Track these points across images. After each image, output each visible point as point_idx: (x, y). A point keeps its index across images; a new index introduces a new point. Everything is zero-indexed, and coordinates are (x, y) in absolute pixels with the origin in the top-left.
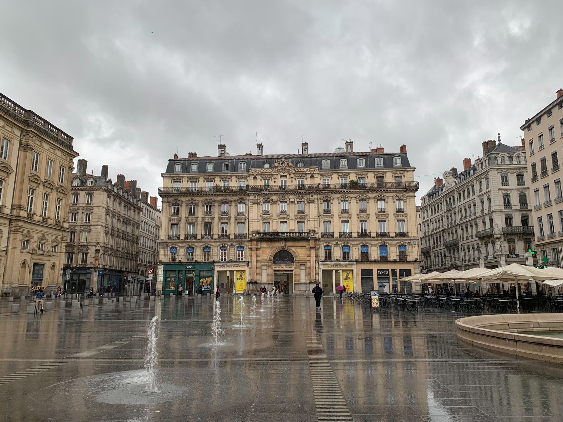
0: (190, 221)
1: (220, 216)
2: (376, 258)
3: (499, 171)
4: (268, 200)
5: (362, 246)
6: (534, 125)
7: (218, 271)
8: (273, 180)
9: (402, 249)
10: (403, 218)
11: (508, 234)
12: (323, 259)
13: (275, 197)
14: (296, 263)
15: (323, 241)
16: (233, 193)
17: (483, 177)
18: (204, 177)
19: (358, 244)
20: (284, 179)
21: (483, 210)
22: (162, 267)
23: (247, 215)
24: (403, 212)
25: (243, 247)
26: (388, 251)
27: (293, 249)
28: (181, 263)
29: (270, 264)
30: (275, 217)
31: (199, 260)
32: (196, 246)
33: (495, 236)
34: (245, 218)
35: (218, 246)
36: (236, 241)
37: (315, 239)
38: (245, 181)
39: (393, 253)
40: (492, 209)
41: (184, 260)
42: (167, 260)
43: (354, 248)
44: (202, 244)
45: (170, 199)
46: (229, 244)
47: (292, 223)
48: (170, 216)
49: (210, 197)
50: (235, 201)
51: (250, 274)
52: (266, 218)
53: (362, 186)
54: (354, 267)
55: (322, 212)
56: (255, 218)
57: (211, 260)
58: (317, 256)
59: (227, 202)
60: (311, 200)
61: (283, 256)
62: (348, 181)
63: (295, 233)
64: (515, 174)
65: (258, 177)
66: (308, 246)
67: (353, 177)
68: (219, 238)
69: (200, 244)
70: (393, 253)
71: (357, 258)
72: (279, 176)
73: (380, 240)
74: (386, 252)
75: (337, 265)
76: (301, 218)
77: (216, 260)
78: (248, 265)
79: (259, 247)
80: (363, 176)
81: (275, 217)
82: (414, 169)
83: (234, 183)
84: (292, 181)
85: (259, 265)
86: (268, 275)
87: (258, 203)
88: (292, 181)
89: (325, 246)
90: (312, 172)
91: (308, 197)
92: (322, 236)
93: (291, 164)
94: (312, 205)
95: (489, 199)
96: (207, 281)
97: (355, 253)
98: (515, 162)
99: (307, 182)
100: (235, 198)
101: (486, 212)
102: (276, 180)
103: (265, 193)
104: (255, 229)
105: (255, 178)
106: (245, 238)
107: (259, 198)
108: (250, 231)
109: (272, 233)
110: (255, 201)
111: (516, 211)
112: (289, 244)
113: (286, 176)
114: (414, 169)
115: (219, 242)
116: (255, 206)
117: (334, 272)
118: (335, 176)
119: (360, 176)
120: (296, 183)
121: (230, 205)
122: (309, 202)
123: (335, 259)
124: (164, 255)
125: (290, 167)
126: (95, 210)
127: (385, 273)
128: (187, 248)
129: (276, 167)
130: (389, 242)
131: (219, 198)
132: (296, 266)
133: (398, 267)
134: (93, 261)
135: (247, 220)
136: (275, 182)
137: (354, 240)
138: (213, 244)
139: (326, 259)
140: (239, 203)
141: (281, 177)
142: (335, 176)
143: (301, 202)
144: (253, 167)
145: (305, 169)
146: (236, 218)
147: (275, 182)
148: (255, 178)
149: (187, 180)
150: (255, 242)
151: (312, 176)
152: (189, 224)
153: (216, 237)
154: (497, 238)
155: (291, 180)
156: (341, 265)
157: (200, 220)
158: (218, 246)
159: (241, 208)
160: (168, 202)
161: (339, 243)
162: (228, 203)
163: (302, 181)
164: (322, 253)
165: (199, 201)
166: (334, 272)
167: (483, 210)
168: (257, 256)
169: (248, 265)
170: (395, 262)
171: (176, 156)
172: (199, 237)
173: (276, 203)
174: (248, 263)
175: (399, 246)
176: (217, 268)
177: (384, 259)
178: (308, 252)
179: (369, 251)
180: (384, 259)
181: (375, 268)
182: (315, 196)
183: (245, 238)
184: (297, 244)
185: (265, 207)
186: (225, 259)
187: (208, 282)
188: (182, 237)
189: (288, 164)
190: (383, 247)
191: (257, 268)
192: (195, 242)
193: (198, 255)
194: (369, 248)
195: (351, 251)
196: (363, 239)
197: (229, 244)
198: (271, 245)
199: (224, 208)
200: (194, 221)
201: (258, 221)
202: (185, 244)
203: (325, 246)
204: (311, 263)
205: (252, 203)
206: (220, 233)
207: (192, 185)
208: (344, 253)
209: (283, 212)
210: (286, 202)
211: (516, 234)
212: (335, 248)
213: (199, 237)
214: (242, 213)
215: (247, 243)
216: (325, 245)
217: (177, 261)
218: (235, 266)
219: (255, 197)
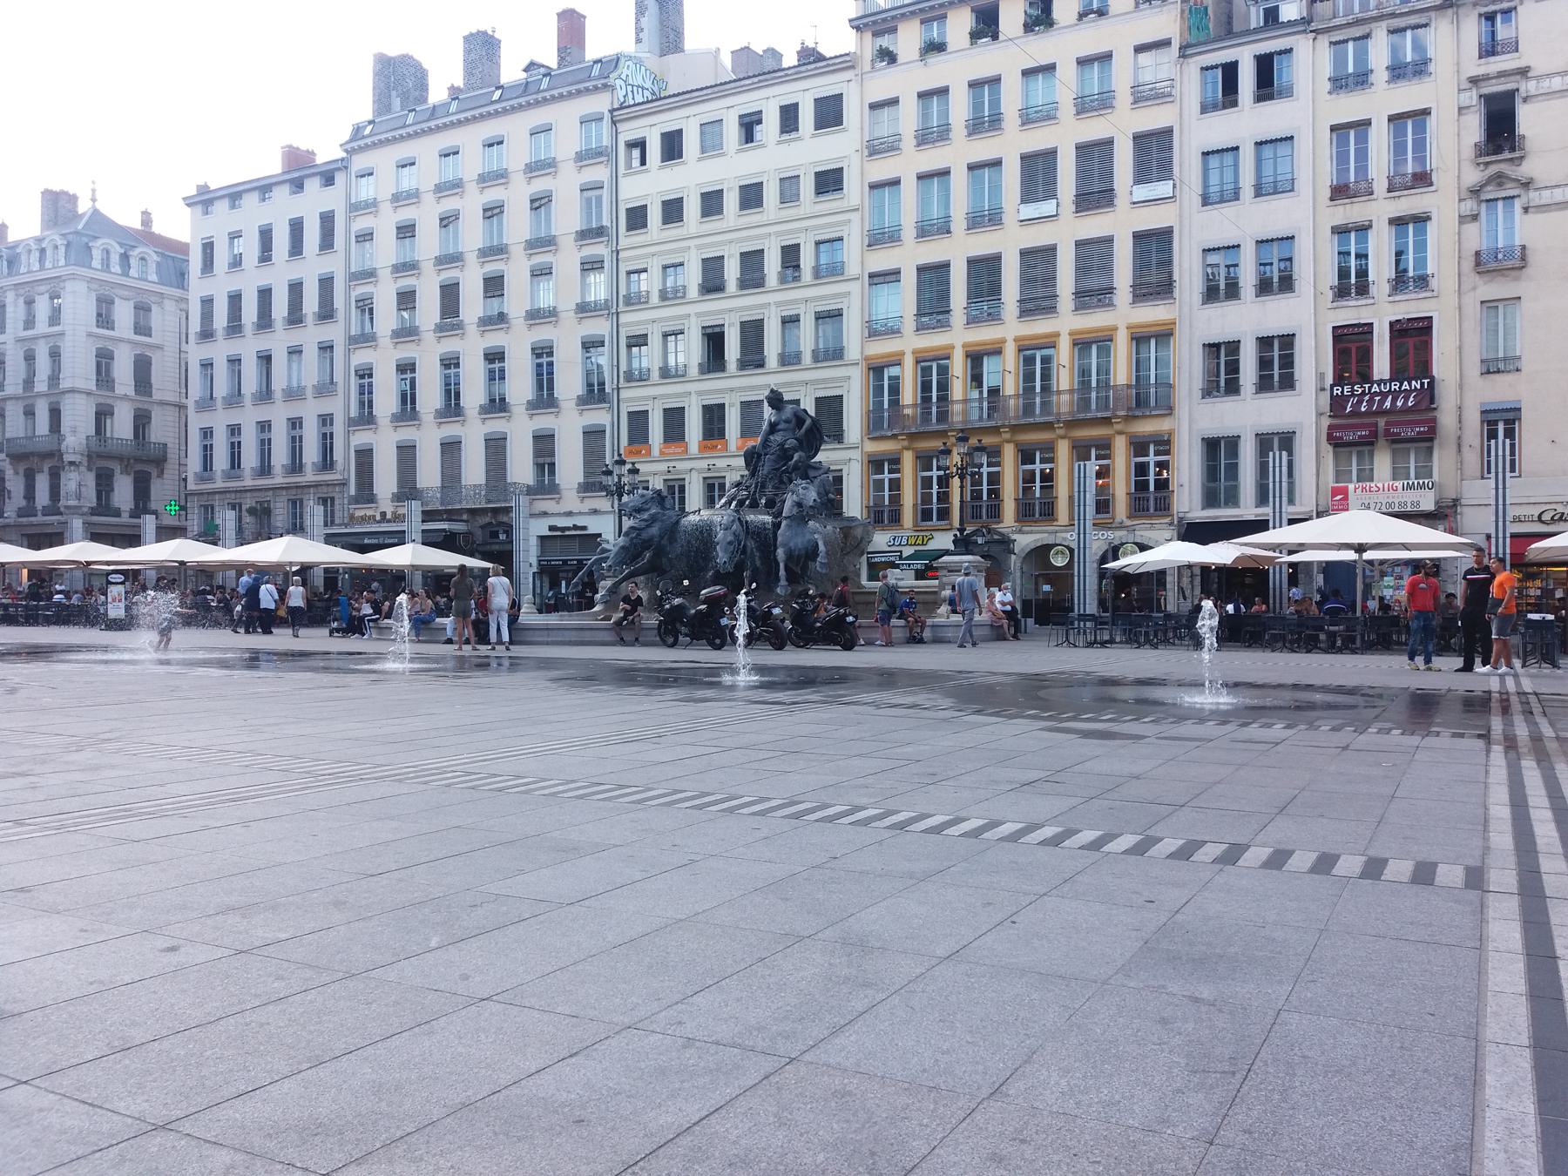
3: (94, 286)
6: (222, 207)
11: (100, 456)
17: (43, 288)
21: (29, 383)
33: (67, 458)
40: (65, 384)
64: (131, 304)
95: (55, 355)
98: (133, 272)
101: (41, 386)
111: (125, 397)
154: (72, 463)
167: (29, 383)
211: (120, 458)
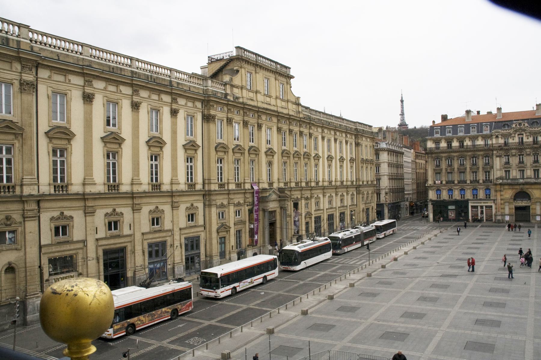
0: (449, 171)
7: (472, 206)
13: (513, 151)
14: (533, 201)
25: (490, 189)
28: (444, 201)
45: (433, 155)
50: (481, 155)
56: (498, 167)
57: (466, 198)
61: (522, 195)
65: (500, 136)
68: (471, 182)
69: (457, 187)
72: (517, 135)
76: (536, 166)
79: (502, 189)
81: (514, 165)
84: (528, 138)
85: (502, 202)
86: (510, 209)
87: (500, 156)
88: (528, 138)
93: (526, 125)
100: (482, 153)
105: (497, 137)
106: (491, 182)
107: (501, 152)
108: (495, 177)
109: (512, 179)
110: (498, 155)
116: (498, 159)
121: (478, 159)
124: (432, 195)
126: (382, 165)
131: (470, 153)
134: (384, 199)
136: (513, 139)
141: (518, 135)
144: (495, 128)
146: (483, 168)
147: (513, 139)
148: (497, 137)
152: (448, 173)
153: (468, 182)
157: (456, 169)
160: (432, 157)
168: (501, 195)
169: (494, 202)
173: (514, 155)
174: (494, 200)
176: (470, 205)
183: (491, 182)
184: (533, 187)
186: (477, 198)
191: (501, 204)
193: (457, 195)
201: (500, 170)
206: (472, 179)
217: (442, 199)
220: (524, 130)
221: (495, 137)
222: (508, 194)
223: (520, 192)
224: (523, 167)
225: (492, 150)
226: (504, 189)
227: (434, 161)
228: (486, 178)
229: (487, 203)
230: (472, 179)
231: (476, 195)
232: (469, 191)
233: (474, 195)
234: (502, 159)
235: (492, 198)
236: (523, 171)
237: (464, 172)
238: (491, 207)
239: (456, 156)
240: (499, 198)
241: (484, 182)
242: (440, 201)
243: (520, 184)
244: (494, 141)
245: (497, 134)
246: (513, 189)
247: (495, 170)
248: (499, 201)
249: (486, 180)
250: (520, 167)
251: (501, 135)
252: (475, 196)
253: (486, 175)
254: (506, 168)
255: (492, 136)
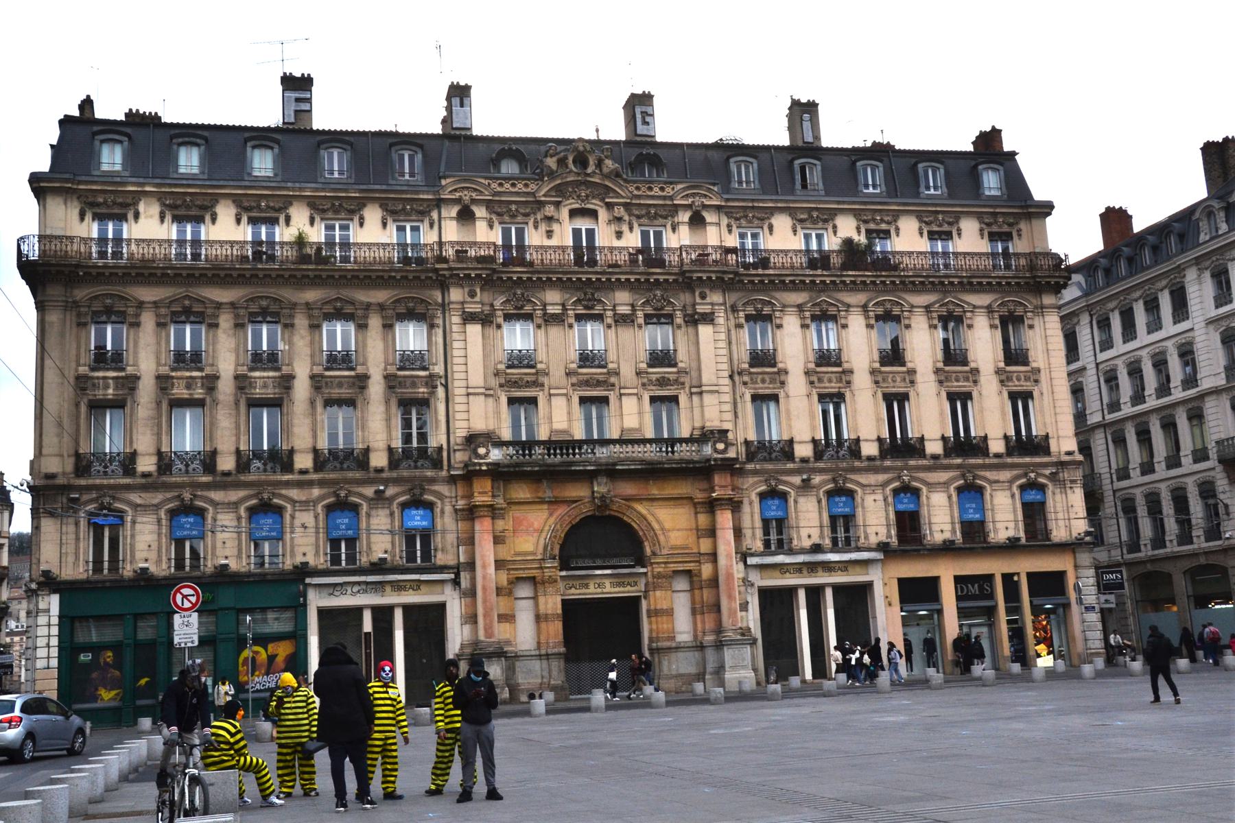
0: (180, 391)
1: (318, 370)
2: (947, 535)
4: (528, 308)
5: (896, 492)
7: (322, 612)
8: (543, 227)
9: (1033, 496)
10: (1026, 386)
12: (759, 545)
13: (553, 297)
15: (755, 472)
16: (371, 276)
18: (237, 201)
19: (884, 485)
20: (584, 224)
22: (53, 602)
23: (439, 369)
24: (1026, 363)
26: (988, 506)
27: (640, 508)
29: (547, 573)
30: (557, 375)
31: (234, 565)
32: (215, 504)
34: (431, 381)
35: (315, 502)
36: (397, 481)
37: (729, 467)
38: (424, 227)
39: (1004, 517)
41: (161, 568)
42: (76, 568)
43: (869, 499)
44: (242, 493)
45: (81, 294)
46: (369, 491)
47: (630, 404)
48: (83, 370)
49: (272, 291)
50: (381, 307)
51: (471, 618)
52: (520, 383)
53: (886, 263)
54: (875, 576)
55: (742, 355)
56: (477, 378)
57: (288, 564)
58: (738, 532)
59: (349, 309)
60: (701, 309)
61: (602, 537)
62: (832, 243)
63: (644, 441)
65: (480, 212)
66: (699, 496)
67: (847, 228)
68: (319, 464)
69: (234, 495)
70: (1004, 517)
71: (883, 538)
72: (564, 213)
73: (958, 467)
74: (982, 509)
75: (812, 567)
76: (663, 382)
77: (317, 560)
78: (456, 582)
79: (500, 501)
80: (884, 226)
81: (557, 375)
82: (1046, 209)
83: (373, 233)
84: (619, 235)
86: (539, 618)
87: (486, 320)
88: (619, 235)
89: (762, 496)
90: (698, 201)
91: (685, 298)
92: (751, 457)
94: (705, 331)
96: (271, 658)
97: (875, 518)
99: (678, 238)
102: (555, 227)
103: (510, 284)
104: (479, 425)
106: (437, 464)
108: (460, 433)
110: (473, 308)
112: (628, 489)
113: (593, 214)
114: (1046, 209)
115: (322, 483)
116: (474, 330)
117: (802, 595)
118: (782, 223)
119: (872, 226)
120: (633, 240)
122: (695, 320)
123: (807, 543)
125: (607, 176)
127: (981, 588)
128: (173, 514)
129: (552, 175)
130: (989, 475)
131: (311, 295)
132: (659, 576)
133: (1024, 566)
135: (441, 392)
136: (549, 234)
137: (867, 470)
138: (294, 493)
139: (767, 544)
140: (402, 317)
141: (573, 213)
142: (782, 223)
143: (658, 317)
145: (669, 191)
146: (391, 381)
147: (549, 234)
149: (155, 209)
150: (487, 484)
151: (697, 221)
153: (303, 461)
155: (613, 228)
156: (828, 567)
157: (226, 387)
158: (315, 502)
159: (411, 337)
161: (817, 479)
162: (348, 317)
163: (658, 236)
164: (752, 515)
165: (219, 306)
166: (802, 595)
168: (498, 540)
169: (456, 582)
170: (1012, 547)
171: (87, 104)
172: (226, 463)
174: (457, 570)
175: (1023, 488)
176: (316, 601)
177: (974, 536)
178: (703, 519)
179: (924, 511)
180: (974, 536)
181: (946, 572)
182: (716, 297)
183: (437, 464)
185: (517, 337)
186: (351, 558)
187: (280, 659)
188: (146, 464)
189: (599, 164)
190: (971, 491)
191: (499, 591)
192: (207, 486)
193: (227, 546)
194: (924, 499)
195: (859, 511)
196: (899, 463)
197: (369, 491)
198: (548, 494)
199: (339, 334)
200: (199, 393)
202: (157, 498)
203: (762, 496)
204: (722, 561)
205: (456, 319)
207: (181, 232)
208: (833, 519)
209: (586, 359)
210: (599, 318)
212: (802, 500)
213: (226, 463)
214: (410, 360)
215: (444, 489)
216: (763, 488)
217: (127, 571)
218: (399, 587)
219: (472, 294)
220: (603, 192)
221: (454, 211)
222: (534, 529)
223: (586, 521)
224: (599, 383)
225: (444, 287)
226: (511, 503)
227: (82, 325)
228: (407, 438)
229: (416, 586)
230: (323, 444)
231: (352, 542)
232: (307, 518)
233: (335, 544)
234: (491, 331)
235: (440, 559)
236: (604, 401)
237: (275, 404)
238: (439, 610)
239: (233, 305)
240: (486, 552)
241: (394, 463)
242: (121, 586)
243: (589, 477)
244: (452, 232)
245: (466, 196)
246: (555, 502)
247: (458, 389)
248: (487, 574)
249: (407, 453)
250: (587, 383)
251: (489, 205)
252: (343, 550)
253: (407, 424)
254: (515, 384)
255: (439, 203)
